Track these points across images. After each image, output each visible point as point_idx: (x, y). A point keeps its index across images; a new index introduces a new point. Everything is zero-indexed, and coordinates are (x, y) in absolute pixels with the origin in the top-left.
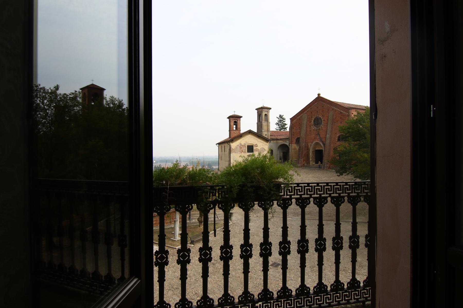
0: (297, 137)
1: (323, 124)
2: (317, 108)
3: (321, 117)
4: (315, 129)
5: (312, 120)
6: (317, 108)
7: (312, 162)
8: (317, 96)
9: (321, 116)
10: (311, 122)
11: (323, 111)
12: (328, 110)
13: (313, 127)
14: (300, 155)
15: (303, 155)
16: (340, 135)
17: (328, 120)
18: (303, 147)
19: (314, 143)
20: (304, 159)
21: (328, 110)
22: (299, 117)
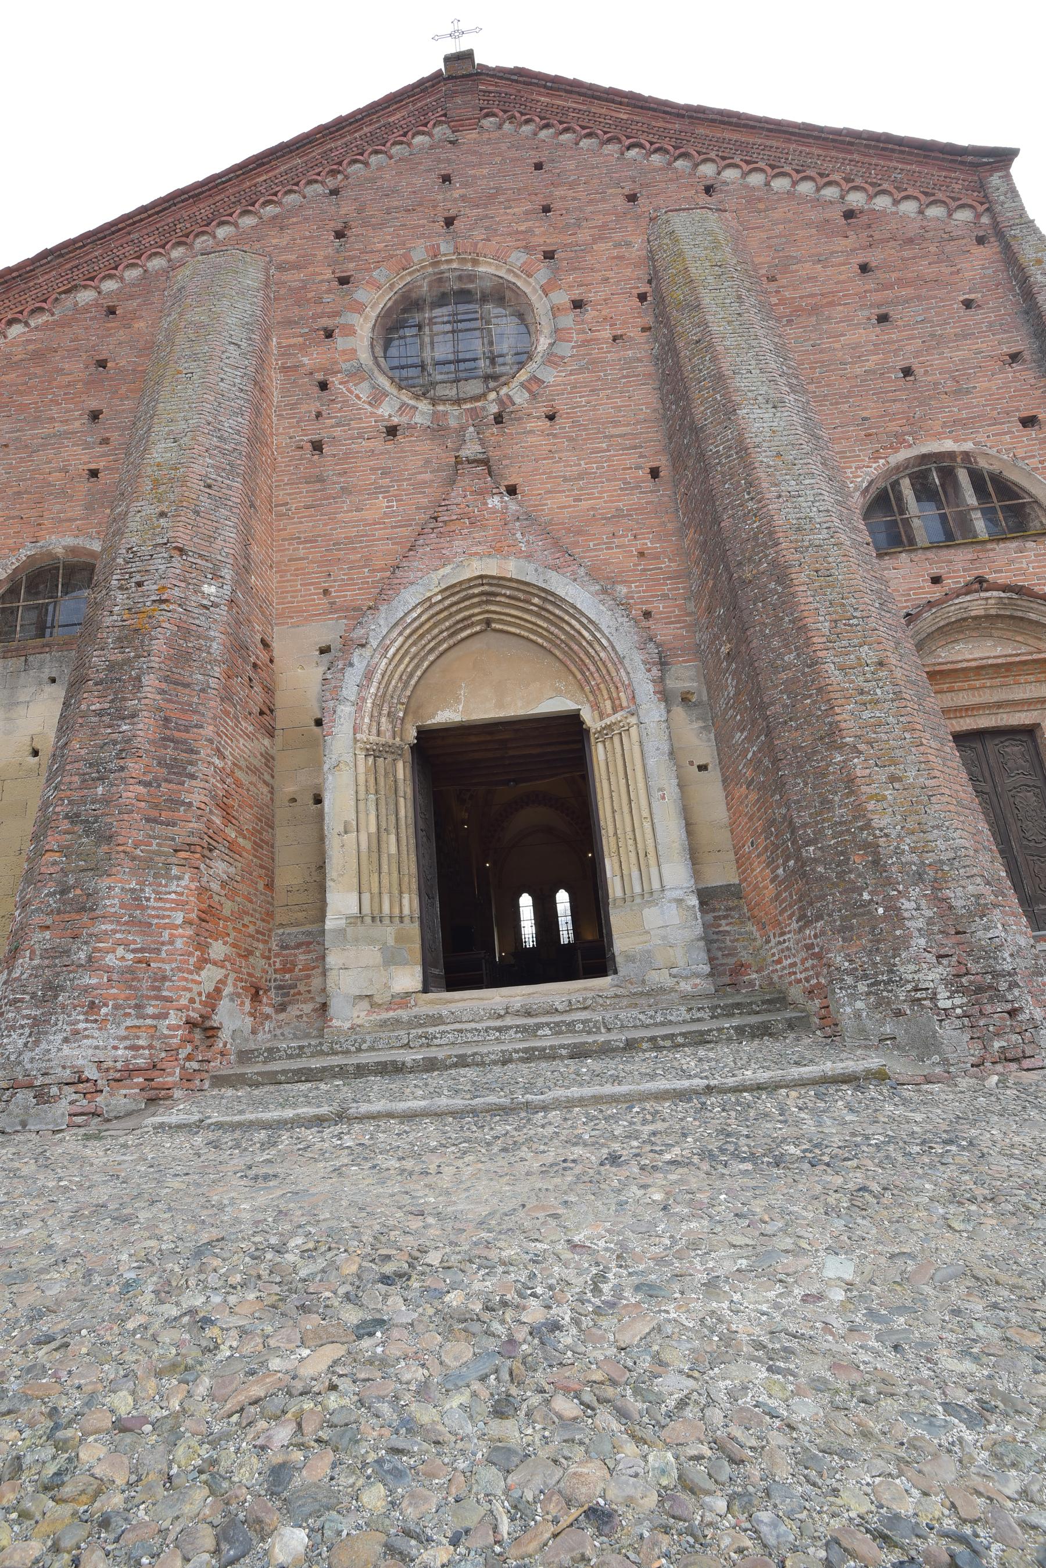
0: (24, 554)
1: (565, 349)
2: (446, 179)
3: (511, 278)
4: (418, 419)
5: (359, 308)
6: (446, 179)
7: (372, 955)
8: (440, 65)
9: (518, 258)
10: (329, 334)
11: (546, 209)
12: (632, 198)
13: (378, 397)
14: (131, 792)
15: (196, 794)
16: (906, 464)
17: (642, 297)
18: (185, 631)
19: (409, 598)
20: (203, 891)
21: (632, 198)
22: (109, 286)
